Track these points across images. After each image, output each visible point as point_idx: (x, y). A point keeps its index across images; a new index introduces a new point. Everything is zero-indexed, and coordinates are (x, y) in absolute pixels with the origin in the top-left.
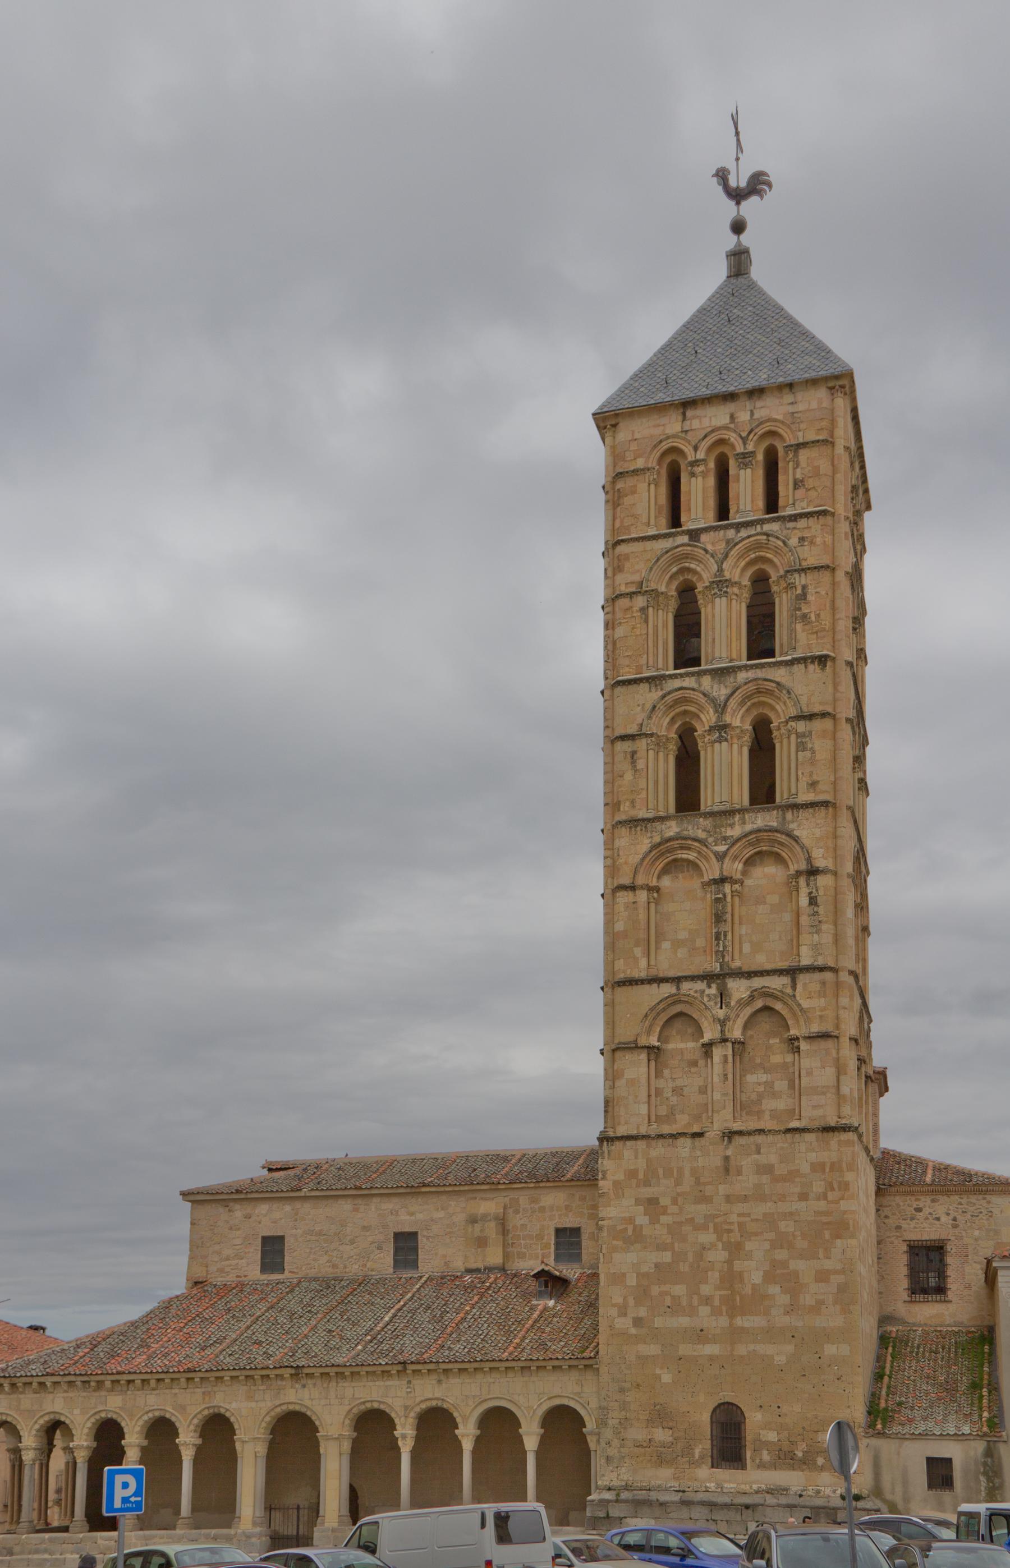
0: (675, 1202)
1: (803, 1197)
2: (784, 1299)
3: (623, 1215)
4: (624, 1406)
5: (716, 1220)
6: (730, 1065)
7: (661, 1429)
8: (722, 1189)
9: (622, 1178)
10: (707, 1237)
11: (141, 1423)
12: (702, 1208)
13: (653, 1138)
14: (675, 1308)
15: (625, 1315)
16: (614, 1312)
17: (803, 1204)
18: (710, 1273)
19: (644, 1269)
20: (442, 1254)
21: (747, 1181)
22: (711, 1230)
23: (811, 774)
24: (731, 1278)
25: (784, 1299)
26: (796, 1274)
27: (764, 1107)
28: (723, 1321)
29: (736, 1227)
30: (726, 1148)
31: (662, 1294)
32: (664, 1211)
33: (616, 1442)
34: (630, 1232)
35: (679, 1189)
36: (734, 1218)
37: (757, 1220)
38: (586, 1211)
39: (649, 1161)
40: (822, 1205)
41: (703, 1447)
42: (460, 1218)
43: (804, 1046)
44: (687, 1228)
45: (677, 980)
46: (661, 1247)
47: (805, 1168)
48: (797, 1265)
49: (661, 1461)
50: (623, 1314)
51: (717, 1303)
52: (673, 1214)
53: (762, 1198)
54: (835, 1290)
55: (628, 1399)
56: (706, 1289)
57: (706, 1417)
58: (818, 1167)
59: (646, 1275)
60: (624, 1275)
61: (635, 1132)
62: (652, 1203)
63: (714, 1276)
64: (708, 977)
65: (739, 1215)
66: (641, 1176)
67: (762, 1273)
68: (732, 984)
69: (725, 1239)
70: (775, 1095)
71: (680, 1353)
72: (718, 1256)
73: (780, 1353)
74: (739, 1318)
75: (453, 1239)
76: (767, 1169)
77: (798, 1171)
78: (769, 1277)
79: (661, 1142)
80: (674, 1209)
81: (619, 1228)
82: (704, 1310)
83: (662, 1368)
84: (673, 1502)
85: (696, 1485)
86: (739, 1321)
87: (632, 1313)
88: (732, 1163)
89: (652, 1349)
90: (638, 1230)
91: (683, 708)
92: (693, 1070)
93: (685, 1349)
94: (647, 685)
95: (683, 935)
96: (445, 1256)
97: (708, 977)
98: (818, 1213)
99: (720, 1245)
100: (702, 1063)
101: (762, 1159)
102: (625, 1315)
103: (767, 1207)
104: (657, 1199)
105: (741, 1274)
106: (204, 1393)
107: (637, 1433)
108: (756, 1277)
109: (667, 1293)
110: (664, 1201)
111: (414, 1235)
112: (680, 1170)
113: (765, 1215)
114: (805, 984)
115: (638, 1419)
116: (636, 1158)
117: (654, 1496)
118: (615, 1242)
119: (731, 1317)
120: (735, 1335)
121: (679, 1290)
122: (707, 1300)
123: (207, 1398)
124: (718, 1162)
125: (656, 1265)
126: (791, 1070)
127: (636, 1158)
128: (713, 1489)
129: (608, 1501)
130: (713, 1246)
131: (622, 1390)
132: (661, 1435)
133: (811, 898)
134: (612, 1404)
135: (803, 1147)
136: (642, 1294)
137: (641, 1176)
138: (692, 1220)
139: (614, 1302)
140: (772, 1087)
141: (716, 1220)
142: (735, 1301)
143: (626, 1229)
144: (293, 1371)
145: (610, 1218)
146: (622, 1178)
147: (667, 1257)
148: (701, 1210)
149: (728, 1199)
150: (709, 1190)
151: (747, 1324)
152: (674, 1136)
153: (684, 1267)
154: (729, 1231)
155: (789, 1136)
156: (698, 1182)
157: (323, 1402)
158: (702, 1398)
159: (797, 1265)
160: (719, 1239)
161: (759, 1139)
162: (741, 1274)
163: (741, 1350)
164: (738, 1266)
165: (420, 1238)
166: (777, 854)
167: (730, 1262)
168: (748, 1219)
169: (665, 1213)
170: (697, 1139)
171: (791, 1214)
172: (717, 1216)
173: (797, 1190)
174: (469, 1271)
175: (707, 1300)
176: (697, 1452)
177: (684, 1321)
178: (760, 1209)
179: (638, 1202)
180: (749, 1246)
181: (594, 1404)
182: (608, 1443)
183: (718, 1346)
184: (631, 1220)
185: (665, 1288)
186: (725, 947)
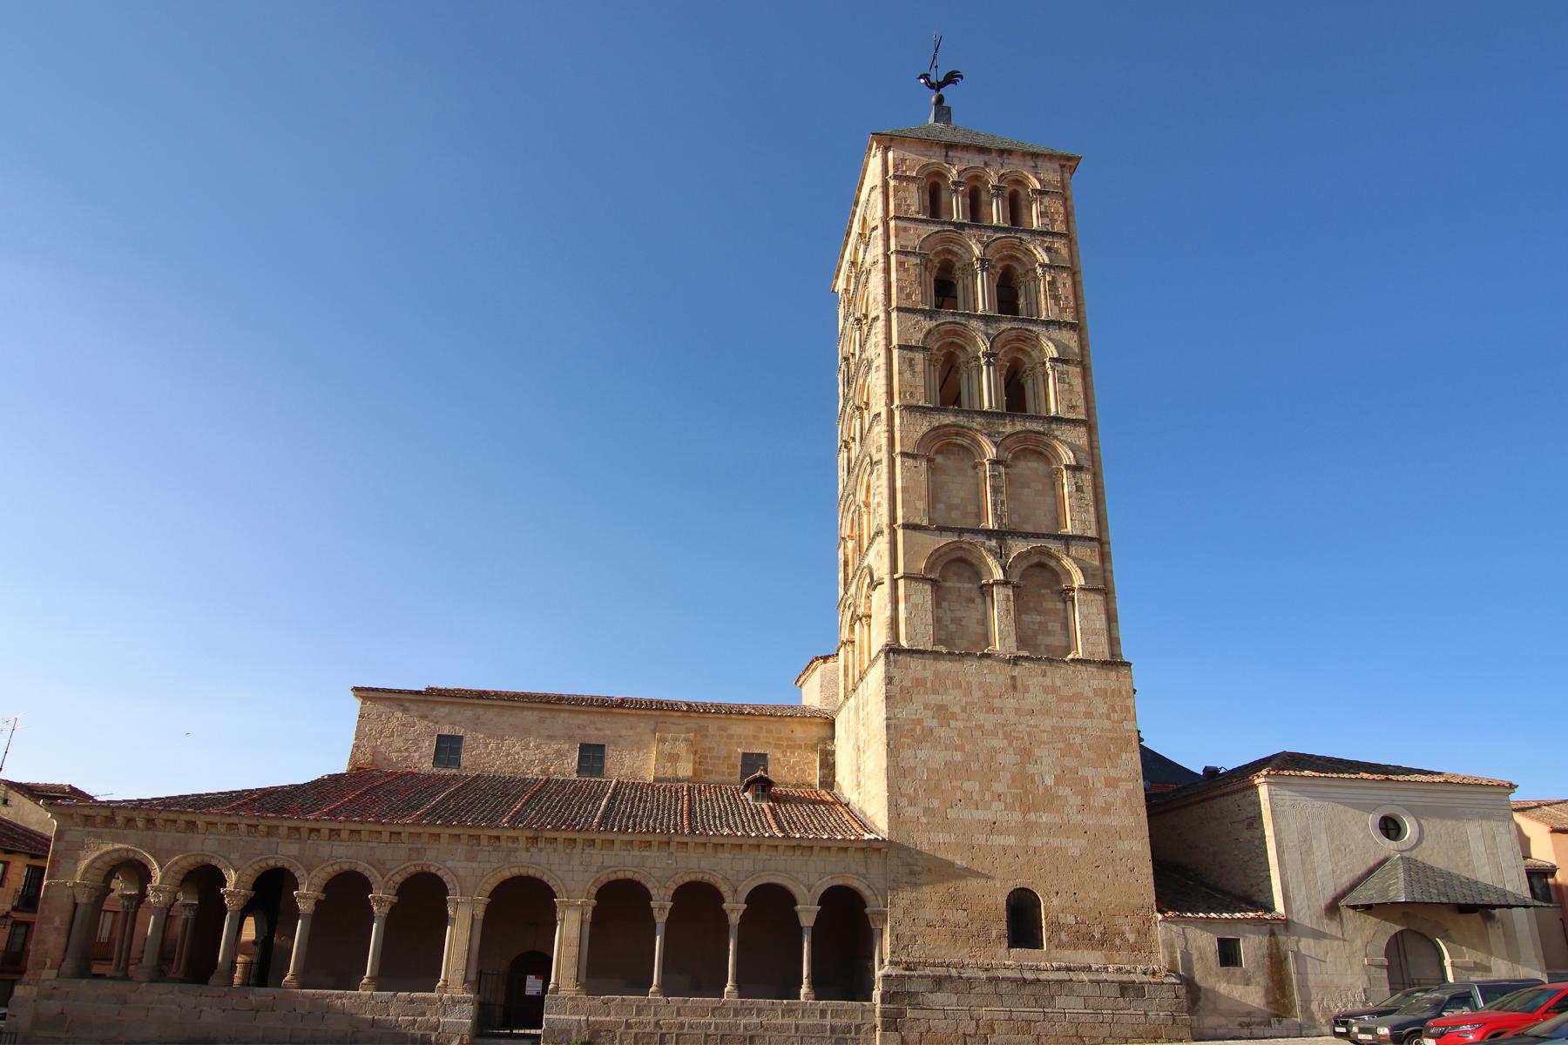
0: (964, 710)
1: (1089, 715)
2: (1078, 800)
8: (1011, 703)
12: (990, 716)
21: (1033, 699)
24: (1023, 780)
25: (1078, 800)
32: (954, 716)
39: (936, 672)
44: (978, 734)
47: (1088, 692)
48: (1089, 772)
53: (1048, 713)
56: (999, 787)
57: (1002, 900)
62: (942, 712)
72: (1008, 759)
73: (1074, 846)
76: (1054, 690)
78: (1058, 781)
82: (996, 805)
86: (1032, 816)
87: (923, 803)
88: (1019, 682)
93: (980, 839)
98: (1102, 730)
101: (1048, 681)
108: (1049, 781)
119: (1024, 813)
120: (1028, 828)
121: (973, 786)
142: (1028, 798)
143: (914, 729)
147: (958, 756)
148: (989, 721)
150: (997, 703)
153: (975, 767)
154: (1017, 739)
156: (987, 695)
159: (1089, 772)
160: (1010, 744)
164: (1030, 769)
177: (979, 814)
178: (1047, 723)
180: (1037, 752)
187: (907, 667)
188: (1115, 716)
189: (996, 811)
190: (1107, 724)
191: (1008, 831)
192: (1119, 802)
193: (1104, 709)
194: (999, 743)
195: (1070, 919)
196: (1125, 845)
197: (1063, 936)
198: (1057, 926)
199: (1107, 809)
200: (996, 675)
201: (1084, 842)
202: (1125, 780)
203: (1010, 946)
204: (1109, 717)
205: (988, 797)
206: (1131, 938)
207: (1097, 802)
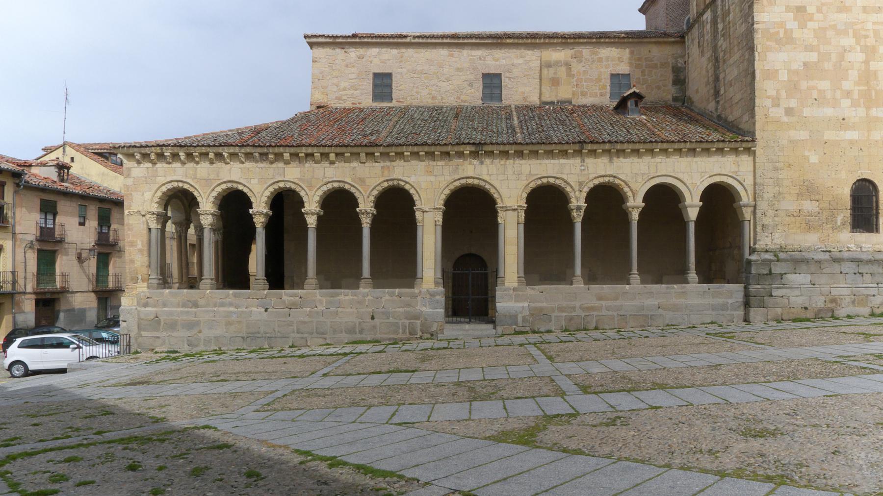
0: (819, 11)
3: (776, 20)
4: (778, 183)
5: (855, 27)
10: (847, 41)
11: (320, 193)
12: (843, 17)
14: (820, 100)
15: (778, 105)
16: (768, 103)
18: (850, 72)
19: (795, 66)
22: (851, 35)
28: (861, 112)
29: (871, 34)
33: (770, 213)
34: (782, 35)
36: (869, 26)
41: (845, 215)
42: (536, 64)
46: (809, 48)
49: (809, 227)
50: (776, 104)
51: (856, 96)
55: (780, 177)
56: (847, 85)
57: (846, 192)
59: (797, 72)
60: (777, 71)
63: (854, 74)
65: (874, 23)
69: (862, 43)
72: (857, 57)
74: (874, 109)
80: (818, 16)
81: (772, 31)
82: (846, 103)
84: (826, 260)
86: (874, 112)
87: (784, 104)
89: (803, 135)
93: (829, 135)
99: (858, 48)
102: (778, 105)
104: (805, 7)
105: (875, 72)
106: (382, 168)
107: (789, 205)
110: (811, 9)
111: (499, 76)
115: (790, 193)
118: (769, 43)
119: (868, 108)
120: (871, 123)
121: (825, 85)
123: (386, 172)
128: (854, 249)
129: (771, 261)
131: (776, 169)
132: (809, 206)
134: (766, 181)
136: (793, 88)
138: (834, 27)
141: (855, 27)
143: (778, 32)
144: (473, 149)
145: (764, 22)
153: (828, 66)
154: (866, 37)
157: (501, 177)
158: (843, 175)
160: (858, 43)
162: (875, 72)
164: (873, 65)
165: (503, 78)
167: (866, 62)
169: (811, 20)
175: (848, 94)
176: (839, 220)
177: (829, 112)
179: (788, 9)
181: (749, 182)
182: (764, 214)
183: (857, 132)
185: (811, 83)
189: (846, 108)
191: (853, 127)
205: (838, 94)
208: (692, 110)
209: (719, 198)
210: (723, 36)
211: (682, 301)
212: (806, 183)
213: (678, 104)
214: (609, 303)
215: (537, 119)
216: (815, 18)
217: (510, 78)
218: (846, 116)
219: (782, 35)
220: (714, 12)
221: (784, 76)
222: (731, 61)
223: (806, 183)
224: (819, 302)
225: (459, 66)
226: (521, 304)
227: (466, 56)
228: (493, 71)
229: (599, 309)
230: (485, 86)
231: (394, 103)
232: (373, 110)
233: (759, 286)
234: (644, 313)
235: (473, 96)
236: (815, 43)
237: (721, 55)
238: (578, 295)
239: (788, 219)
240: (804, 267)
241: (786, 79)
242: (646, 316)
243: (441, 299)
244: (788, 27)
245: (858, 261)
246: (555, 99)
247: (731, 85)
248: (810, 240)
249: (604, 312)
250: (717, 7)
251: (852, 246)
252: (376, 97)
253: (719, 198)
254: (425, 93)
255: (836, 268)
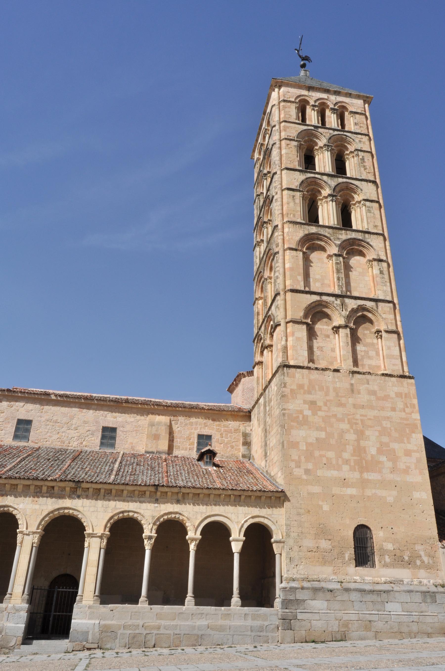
0: (325, 404)
1: (393, 409)
5: (349, 417)
6: (349, 339)
7: (324, 541)
8: (351, 401)
9: (295, 388)
10: (345, 426)
12: (341, 409)
13: (312, 369)
14: (328, 465)
17: (393, 413)
18: (347, 446)
19: (310, 440)
20: (126, 443)
23: (374, 222)
25: (389, 464)
26: (394, 450)
27: (365, 363)
28: (357, 475)
29: (360, 423)
30: (351, 379)
31: (321, 456)
32: (320, 409)
33: (296, 548)
34: (301, 418)
35: (328, 398)
36: (358, 417)
37: (370, 419)
38: (215, 427)
39: (310, 381)
40: (403, 415)
41: (350, 553)
43: (384, 334)
44: (333, 420)
45: (321, 294)
47: (393, 395)
48: (395, 446)
49: (324, 562)
51: (352, 464)
52: (325, 411)
53: (372, 408)
54: (415, 461)
55: (303, 520)
56: (346, 455)
57: (350, 533)
58: (399, 395)
59: (311, 444)
60: (298, 443)
61: (302, 365)
63: (350, 448)
64: (336, 296)
65: (361, 415)
66: (306, 388)
67: (376, 449)
68: (347, 300)
70: (370, 358)
71: (333, 492)
72: (351, 437)
73: (390, 496)
74: (365, 474)
75: (138, 434)
76: (373, 393)
77: (389, 395)
78: (380, 451)
79: (316, 371)
80: (325, 408)
81: (294, 415)
82: (346, 468)
83: (323, 501)
84: (338, 590)
85: (348, 578)
86: (366, 475)
89: (316, 489)
90: (305, 418)
91: (313, 187)
92: (328, 339)
93: (336, 490)
94: (299, 173)
95: (318, 277)
96: (132, 443)
97: (336, 296)
98: (401, 419)
99: (352, 431)
100: (332, 336)
101: (371, 387)
103: (375, 413)
104: (315, 402)
105: (364, 448)
107: (309, 543)
108: (373, 451)
109: (324, 456)
110: (320, 403)
112: (328, 388)
113: (374, 416)
114: (382, 307)
115: (310, 533)
116: (303, 378)
117: (323, 585)
118: (292, 423)
119: (361, 473)
120: (364, 483)
121: (331, 454)
122: (347, 462)
124: (348, 386)
125: (317, 439)
126: (376, 347)
127: (303, 378)
128: (359, 581)
129: (296, 588)
130: (348, 431)
132: (324, 544)
133: (380, 271)
134: (292, 523)
135: (390, 384)
136: (309, 455)
137: (306, 388)
138: (335, 416)
139: (293, 458)
140: (368, 354)
141: (349, 417)
142: (363, 464)
143: (298, 417)
145: (289, 409)
146: (295, 388)
148: (339, 411)
149: (355, 406)
150: (343, 400)
151: (370, 478)
152: (323, 369)
153: (333, 442)
154: (356, 424)
155: (383, 377)
156: (337, 395)
157: (92, 509)
158: (348, 521)
159: (395, 446)
160: (352, 427)
161: (368, 377)
162: (364, 448)
163: (369, 492)
164: (362, 443)
166: (361, 251)
167: (358, 441)
168: (365, 418)
169: (320, 409)
170: (335, 373)
171: (388, 418)
172: (349, 415)
173: (390, 405)
174: (147, 452)
175: (347, 462)
176: (347, 556)
177: (334, 473)
178: (372, 413)
179: (305, 402)
180: (367, 433)
184: (301, 412)
185: (323, 453)
186: (342, 284)
187: (294, 377)
188: (407, 410)
189: (345, 471)
190: (403, 415)
192: (413, 466)
193: (400, 405)
194: (345, 426)
195: (390, 546)
196: (417, 495)
197: (387, 559)
198: (383, 552)
199: (406, 471)
200: (343, 382)
201: (394, 493)
202: (414, 451)
203: (356, 566)
204: (404, 411)
205: (340, 461)
206: (426, 559)
207: (401, 466)
208: (253, 465)
209: (259, 536)
210: (269, 415)
211: (227, 622)
212: (321, 526)
213: (245, 460)
214: (168, 623)
215: (135, 464)
216: (323, 409)
217: (123, 432)
218: (347, 477)
219: (301, 418)
220: (265, 398)
221: (303, 447)
222: (272, 433)
223: (321, 526)
224: (334, 626)
225: (85, 419)
226: (93, 622)
227: (90, 415)
228: (111, 425)
229: (159, 628)
230: (103, 437)
231: (30, 444)
232: (11, 448)
233: (287, 611)
234: (195, 632)
235: (93, 443)
236: (323, 426)
237: (268, 428)
238: (143, 614)
239: (309, 553)
240: (321, 594)
241: (305, 449)
242: (198, 636)
243: (24, 615)
244: (305, 414)
245: (362, 591)
246: (154, 450)
247: (272, 450)
248: (326, 574)
249: (162, 631)
250: (266, 395)
251: (357, 578)
252: (16, 437)
253: (259, 536)
254: (55, 437)
255: (345, 597)
